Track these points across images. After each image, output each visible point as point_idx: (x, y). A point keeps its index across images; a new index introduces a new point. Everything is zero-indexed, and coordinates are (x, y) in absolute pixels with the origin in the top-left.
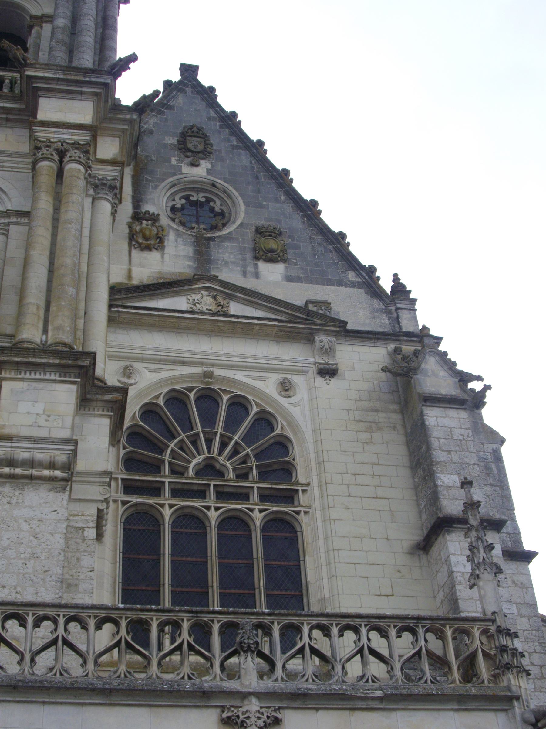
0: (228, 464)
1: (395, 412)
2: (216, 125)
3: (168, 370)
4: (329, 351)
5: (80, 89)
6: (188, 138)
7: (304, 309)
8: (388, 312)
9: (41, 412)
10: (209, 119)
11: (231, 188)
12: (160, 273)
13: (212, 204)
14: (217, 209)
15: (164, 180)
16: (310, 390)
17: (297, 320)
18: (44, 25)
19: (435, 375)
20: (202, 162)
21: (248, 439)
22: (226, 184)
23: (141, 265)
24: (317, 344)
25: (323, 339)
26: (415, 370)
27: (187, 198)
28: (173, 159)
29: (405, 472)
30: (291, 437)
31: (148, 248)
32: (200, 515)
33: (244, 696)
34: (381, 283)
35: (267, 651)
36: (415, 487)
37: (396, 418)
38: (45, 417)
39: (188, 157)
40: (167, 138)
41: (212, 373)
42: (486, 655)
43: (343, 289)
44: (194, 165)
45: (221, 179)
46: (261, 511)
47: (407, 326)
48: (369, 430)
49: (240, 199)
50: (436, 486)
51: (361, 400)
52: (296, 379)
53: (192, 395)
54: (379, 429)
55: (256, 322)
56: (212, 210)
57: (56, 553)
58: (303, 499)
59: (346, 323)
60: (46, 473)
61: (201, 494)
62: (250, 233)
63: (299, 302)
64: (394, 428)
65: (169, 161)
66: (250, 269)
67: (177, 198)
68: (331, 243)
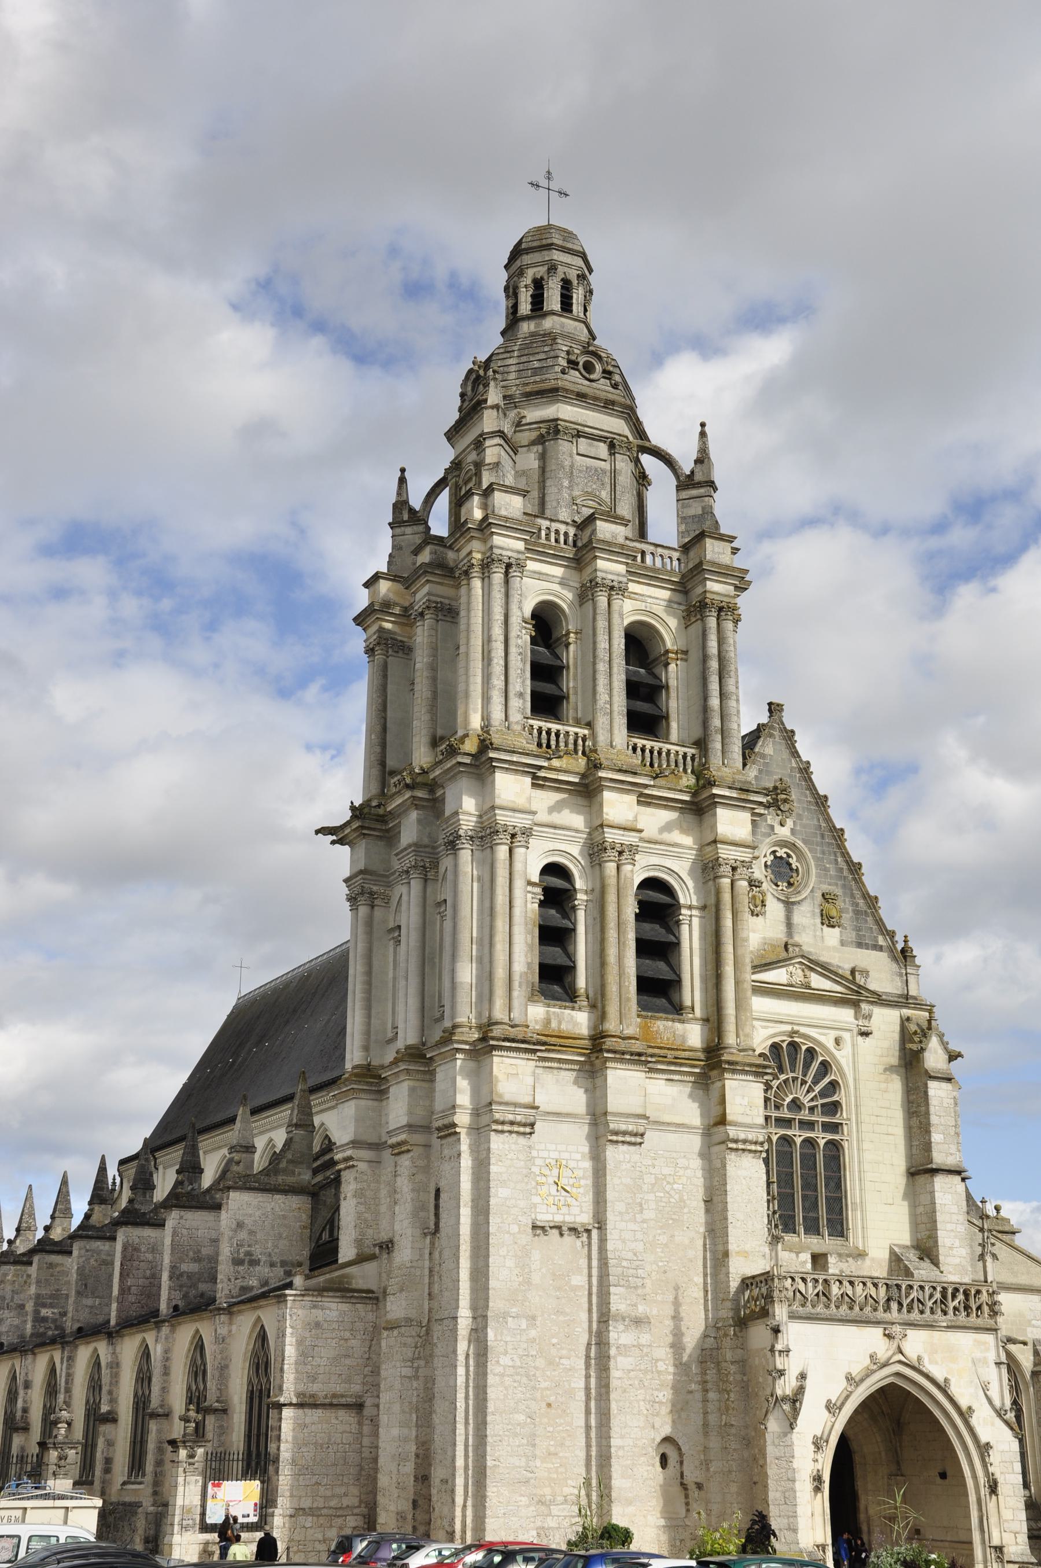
4: (869, 1017)
8: (901, 975)
10: (792, 769)
11: (806, 849)
12: (764, 938)
19: (936, 1052)
30: (840, 1082)
31: (757, 915)
32: (790, 1140)
34: (897, 945)
38: (749, 1108)
39: (778, 815)
42: (987, 1304)
43: (874, 952)
45: (799, 839)
49: (812, 861)
50: (930, 1140)
52: (846, 1036)
56: (790, 865)
58: (845, 1127)
60: (753, 1147)
62: (818, 895)
66: (819, 933)
67: (768, 854)
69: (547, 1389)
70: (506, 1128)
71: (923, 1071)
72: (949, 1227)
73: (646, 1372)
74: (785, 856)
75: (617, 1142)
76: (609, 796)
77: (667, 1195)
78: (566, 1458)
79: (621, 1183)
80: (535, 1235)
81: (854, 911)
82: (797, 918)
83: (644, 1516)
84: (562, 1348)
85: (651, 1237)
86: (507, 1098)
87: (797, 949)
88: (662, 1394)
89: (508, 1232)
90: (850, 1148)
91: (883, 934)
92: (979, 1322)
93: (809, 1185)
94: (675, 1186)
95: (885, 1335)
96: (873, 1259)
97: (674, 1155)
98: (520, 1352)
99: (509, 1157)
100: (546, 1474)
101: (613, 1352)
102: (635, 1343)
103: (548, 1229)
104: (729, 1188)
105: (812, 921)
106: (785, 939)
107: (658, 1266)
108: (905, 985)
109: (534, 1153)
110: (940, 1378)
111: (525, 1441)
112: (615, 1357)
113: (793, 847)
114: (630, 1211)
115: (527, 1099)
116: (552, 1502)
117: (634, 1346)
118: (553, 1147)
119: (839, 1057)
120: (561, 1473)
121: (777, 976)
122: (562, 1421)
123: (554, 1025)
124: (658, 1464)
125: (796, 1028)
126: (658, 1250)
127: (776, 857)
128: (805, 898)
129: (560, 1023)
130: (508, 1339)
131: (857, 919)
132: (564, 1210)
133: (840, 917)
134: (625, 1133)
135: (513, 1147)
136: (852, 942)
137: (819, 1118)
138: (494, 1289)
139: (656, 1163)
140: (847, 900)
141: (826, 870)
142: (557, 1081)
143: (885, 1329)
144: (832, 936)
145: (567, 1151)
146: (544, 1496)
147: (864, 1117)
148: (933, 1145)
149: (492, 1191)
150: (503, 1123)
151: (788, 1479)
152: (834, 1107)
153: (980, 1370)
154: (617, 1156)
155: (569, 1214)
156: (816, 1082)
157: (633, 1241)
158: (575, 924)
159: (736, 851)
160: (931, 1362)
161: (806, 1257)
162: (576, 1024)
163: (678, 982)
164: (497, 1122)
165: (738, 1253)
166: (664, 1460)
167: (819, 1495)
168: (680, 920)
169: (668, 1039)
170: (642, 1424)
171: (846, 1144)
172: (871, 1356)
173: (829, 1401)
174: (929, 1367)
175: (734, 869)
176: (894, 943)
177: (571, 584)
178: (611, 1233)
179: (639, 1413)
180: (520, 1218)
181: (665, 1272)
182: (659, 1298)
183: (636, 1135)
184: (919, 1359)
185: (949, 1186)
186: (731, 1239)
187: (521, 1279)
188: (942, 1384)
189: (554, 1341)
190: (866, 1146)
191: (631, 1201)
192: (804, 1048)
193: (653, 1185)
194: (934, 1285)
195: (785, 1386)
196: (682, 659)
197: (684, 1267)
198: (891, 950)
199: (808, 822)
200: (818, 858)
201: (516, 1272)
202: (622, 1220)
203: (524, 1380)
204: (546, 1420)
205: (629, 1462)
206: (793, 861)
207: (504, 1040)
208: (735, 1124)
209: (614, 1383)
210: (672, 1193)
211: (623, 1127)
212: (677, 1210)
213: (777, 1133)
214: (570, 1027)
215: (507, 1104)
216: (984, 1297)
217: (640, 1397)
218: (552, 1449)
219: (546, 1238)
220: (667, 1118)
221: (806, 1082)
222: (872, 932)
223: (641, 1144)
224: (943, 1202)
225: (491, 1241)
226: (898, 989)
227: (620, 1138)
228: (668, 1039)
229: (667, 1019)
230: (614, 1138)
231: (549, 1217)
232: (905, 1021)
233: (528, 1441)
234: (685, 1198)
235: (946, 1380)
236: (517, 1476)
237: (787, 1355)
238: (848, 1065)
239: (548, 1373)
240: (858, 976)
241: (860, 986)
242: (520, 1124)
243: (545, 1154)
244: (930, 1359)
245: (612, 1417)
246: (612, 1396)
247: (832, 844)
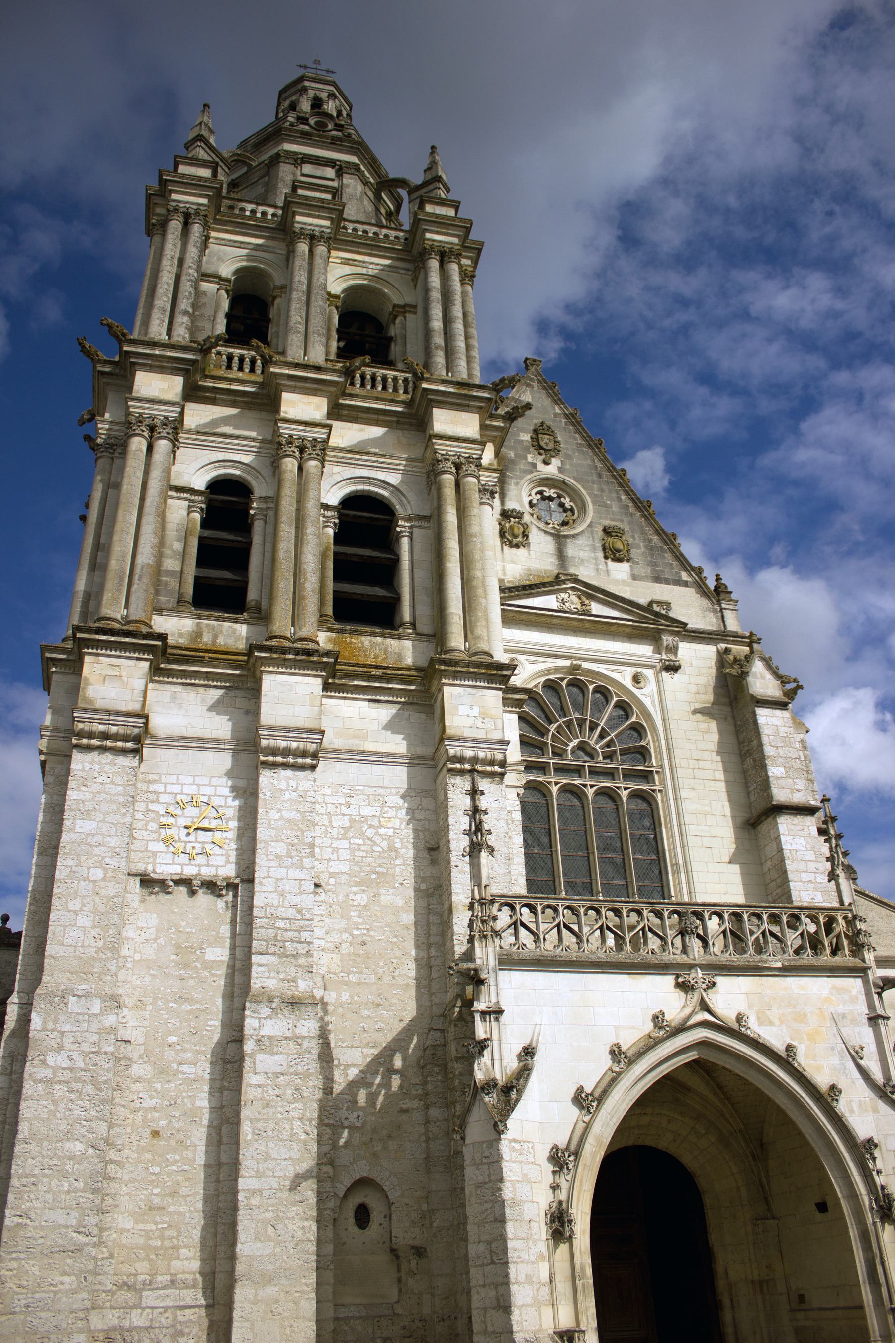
0: (597, 747)
1: (725, 705)
2: (561, 421)
3: (544, 662)
4: (674, 650)
5: (467, 403)
6: (540, 436)
7: (648, 608)
8: (715, 611)
9: (477, 715)
11: (579, 487)
12: (529, 569)
13: (562, 500)
14: (567, 506)
15: (523, 477)
16: (658, 682)
17: (644, 620)
18: (407, 315)
19: (763, 677)
20: (553, 459)
22: (575, 483)
25: (667, 639)
28: (529, 456)
31: (517, 546)
33: (691, 967)
34: (707, 582)
35: (701, 933)
38: (480, 719)
39: (540, 454)
40: (521, 434)
41: (580, 666)
42: (847, 936)
43: (677, 588)
44: (546, 463)
45: (569, 477)
46: (625, 789)
51: (699, 694)
55: (614, 621)
56: (562, 505)
57: (502, 836)
59: (686, 624)
61: (578, 771)
62: (599, 530)
63: (643, 601)
65: (526, 458)
66: (602, 566)
69: (154, 1109)
70: (94, 742)
71: (748, 699)
72: (805, 877)
73: (306, 1076)
74: (555, 496)
76: (286, 396)
77: (369, 842)
78: (180, 1213)
79: (282, 817)
80: (151, 893)
81: (646, 547)
82: (571, 550)
83: (295, 1303)
84: (184, 1050)
86: (99, 704)
88: (355, 1114)
90: (666, 799)
91: (686, 570)
92: (837, 960)
94: (382, 831)
95: (678, 985)
98: (86, 1047)
99: (100, 780)
100: (141, 1240)
101: (249, 1046)
102: (289, 1034)
103: (171, 884)
105: (592, 555)
106: (556, 571)
107: (351, 934)
108: (721, 621)
110: (779, 1046)
111: (81, 1185)
112: (252, 1055)
113: (563, 487)
114: (294, 853)
115: (135, 707)
116: (149, 1285)
117: (286, 1038)
118: (190, 780)
119: (639, 696)
120: (170, 1238)
122: (177, 1157)
124: (352, 1220)
126: (352, 913)
128: (582, 532)
129: (216, 636)
130: (66, 1028)
131: (652, 555)
132: (201, 859)
133: (628, 551)
134: (287, 752)
135: (108, 768)
136: (647, 577)
138: (53, 957)
139: (352, 801)
140: (636, 536)
141: (606, 506)
143: (678, 976)
145: (210, 785)
146: (135, 1275)
148: (771, 779)
149: (67, 823)
151: (496, 1220)
153: (843, 1030)
154: (276, 782)
155: (208, 865)
157: (296, 894)
159: (459, 447)
160: (761, 1023)
164: (80, 734)
166: (362, 1216)
167: (564, 1247)
169: (376, 657)
170: (295, 1155)
172: (655, 1018)
173: (581, 1090)
174: (755, 1028)
175: (458, 466)
177: (279, 251)
178: (261, 884)
179: (293, 1137)
180: (108, 860)
181: (364, 943)
182: (353, 978)
184: (739, 1018)
185: (800, 827)
187: (101, 943)
188: (783, 1054)
189: (172, 1039)
190: (684, 794)
191: (296, 841)
192: (591, 688)
193: (347, 829)
194: (758, 911)
196: (409, 312)
197: (396, 936)
199: (579, 461)
200: (596, 496)
201: (93, 933)
202: (280, 866)
203: (90, 1089)
204: (148, 1156)
205: (270, 1215)
209: (249, 1093)
210: (377, 839)
212: (385, 861)
216: (841, 925)
217: (295, 1114)
218: (156, 1201)
219: (168, 897)
221: (598, 725)
222: (672, 568)
224: (794, 847)
225: (55, 890)
226: (713, 626)
227: (279, 759)
228: (376, 657)
229: (375, 634)
231: (178, 870)
233: (86, 1184)
234: (398, 845)
235: (789, 1048)
236: (60, 1241)
237: (497, 1019)
238: (654, 705)
239: (158, 1086)
240: (655, 606)
241: (657, 614)
242: (115, 737)
243: (177, 789)
244: (758, 1018)
245: (242, 1145)
246: (245, 1113)
247: (612, 483)
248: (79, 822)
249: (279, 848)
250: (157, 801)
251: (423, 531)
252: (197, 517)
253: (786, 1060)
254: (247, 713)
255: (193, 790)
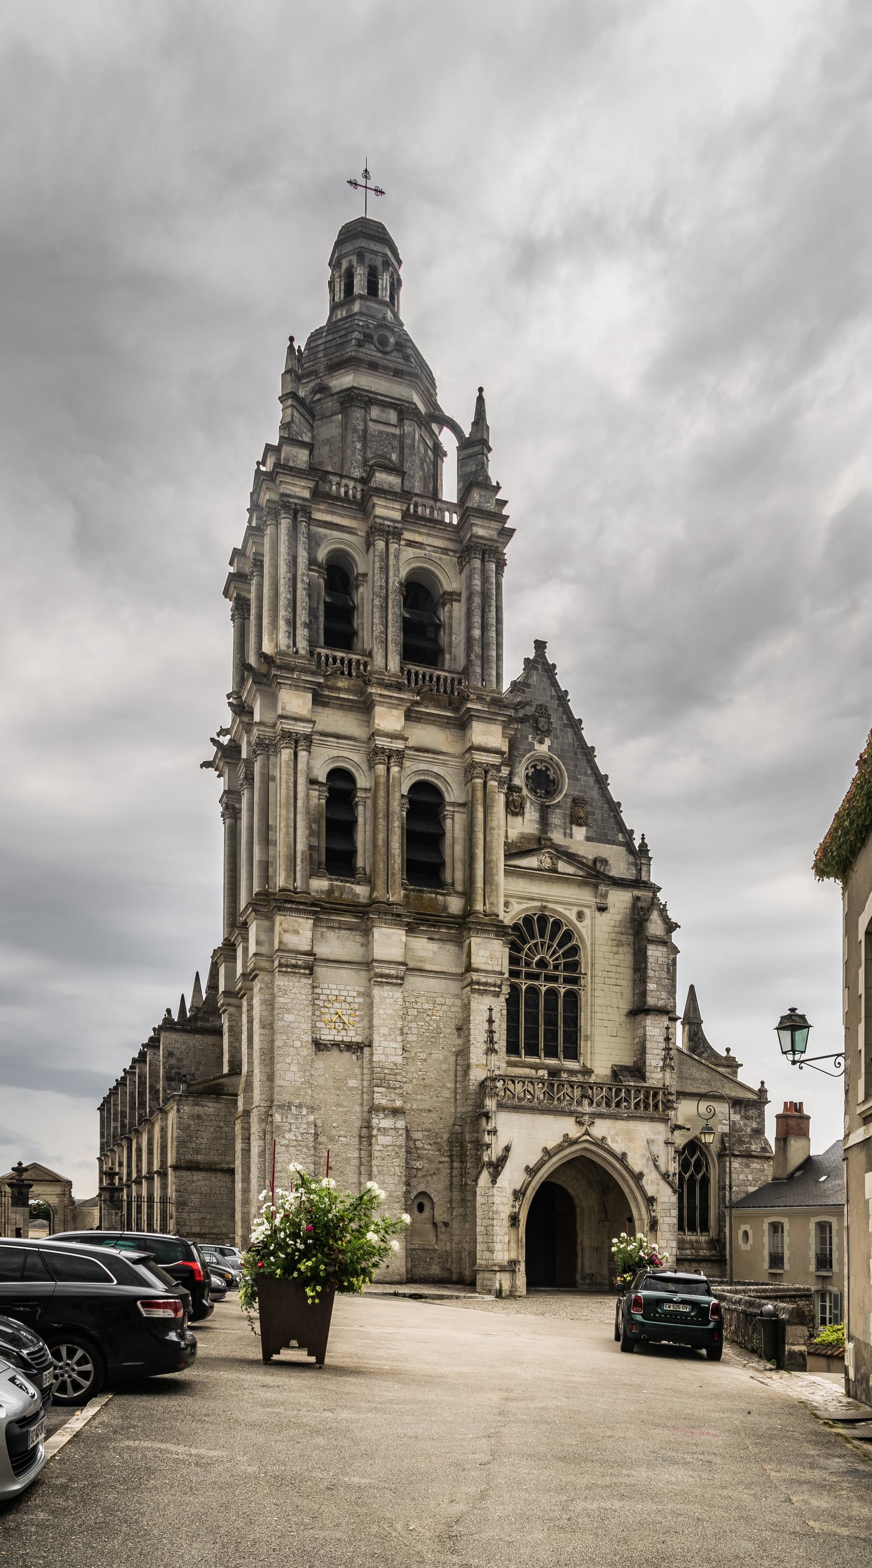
4: (605, 896)
8: (636, 865)
12: (522, 833)
14: (551, 777)
16: (592, 918)
19: (656, 923)
20: (546, 739)
21: (560, 945)
23: (513, 828)
24: (600, 892)
25: (602, 888)
26: (646, 920)
27: (534, 766)
28: (530, 736)
29: (630, 971)
36: (634, 981)
37: (631, 938)
43: (615, 847)
44: (541, 742)
47: (644, 878)
48: (618, 945)
52: (587, 911)
53: (535, 918)
54: (623, 945)
56: (549, 776)
58: (583, 982)
60: (492, 989)
61: (536, 977)
62: (569, 800)
64: (629, 945)
66: (568, 831)
68: (612, 811)
74: (544, 769)
75: (382, 982)
85: (413, 1055)
87: (548, 843)
89: (293, 1046)
91: (622, 832)
93: (551, 1021)
94: (434, 1018)
96: (597, 1076)
97: (434, 995)
99: (293, 991)
104: (471, 1018)
109: (318, 991)
118: (331, 986)
121: (530, 862)
123: (337, 894)
125: (544, 904)
127: (536, 769)
129: (342, 894)
133: (587, 818)
135: (297, 984)
137: (562, 974)
142: (338, 937)
144: (580, 833)
147: (598, 972)
150: (287, 966)
152: (574, 966)
156: (560, 945)
158: (356, 818)
161: (543, 1073)
162: (357, 895)
163: (441, 865)
165: (477, 1066)
168: (445, 815)
171: (582, 993)
176: (632, 839)
183: (397, 978)
186: (472, 1056)
192: (551, 920)
195: (494, 1154)
198: (628, 845)
206: (551, 774)
207: (286, 901)
208: (477, 970)
211: (387, 971)
213: (524, 984)
214: (350, 897)
215: (290, 951)
220: (428, 967)
223: (401, 984)
227: (384, 980)
230: (379, 979)
232: (637, 899)
238: (587, 933)
240: (598, 865)
241: (598, 872)
248: (286, 1016)
249: (384, 1030)
250: (318, 999)
251: (460, 815)
252: (323, 801)
253: (622, 1159)
254: (362, 945)
255: (336, 992)
